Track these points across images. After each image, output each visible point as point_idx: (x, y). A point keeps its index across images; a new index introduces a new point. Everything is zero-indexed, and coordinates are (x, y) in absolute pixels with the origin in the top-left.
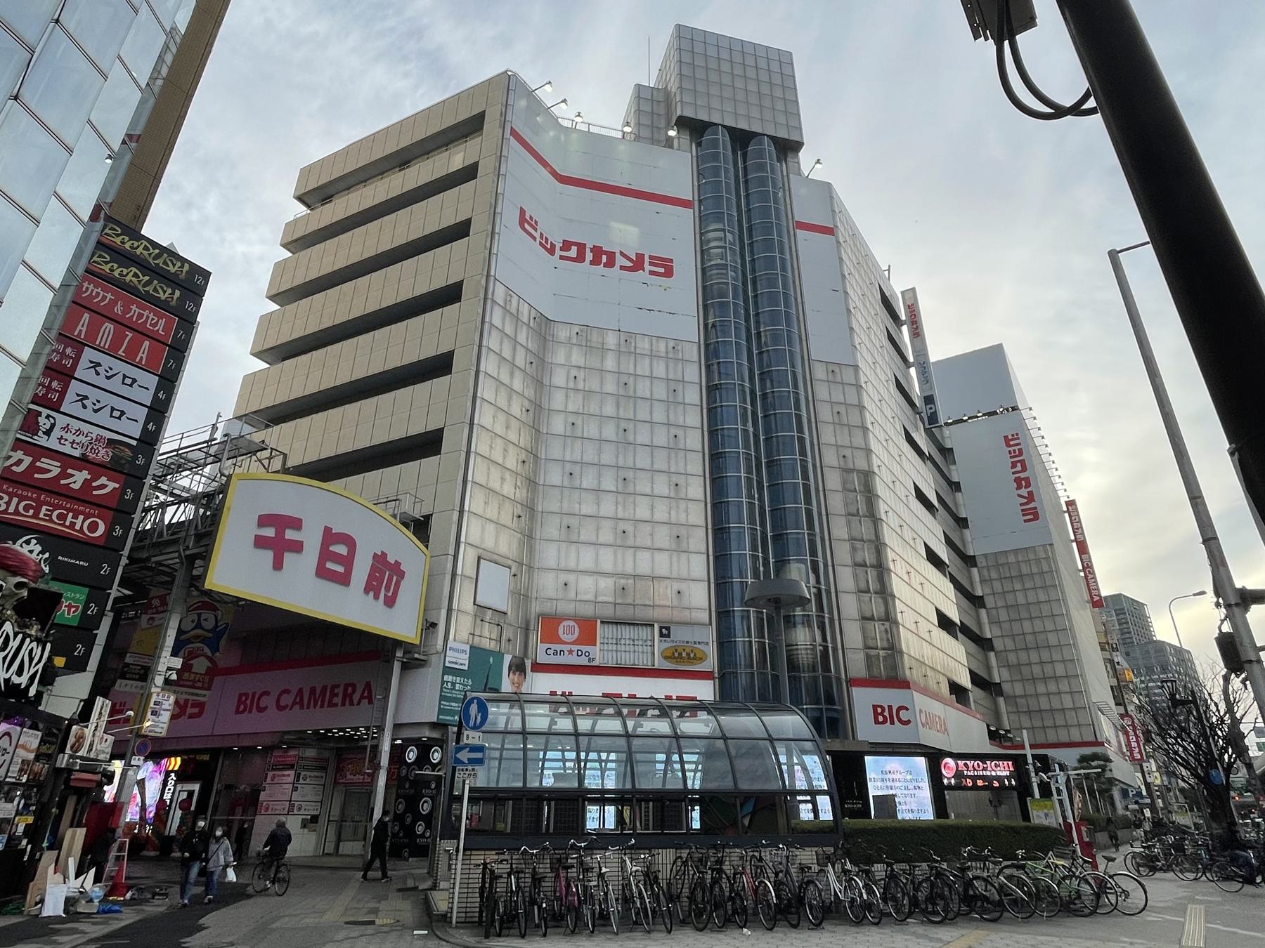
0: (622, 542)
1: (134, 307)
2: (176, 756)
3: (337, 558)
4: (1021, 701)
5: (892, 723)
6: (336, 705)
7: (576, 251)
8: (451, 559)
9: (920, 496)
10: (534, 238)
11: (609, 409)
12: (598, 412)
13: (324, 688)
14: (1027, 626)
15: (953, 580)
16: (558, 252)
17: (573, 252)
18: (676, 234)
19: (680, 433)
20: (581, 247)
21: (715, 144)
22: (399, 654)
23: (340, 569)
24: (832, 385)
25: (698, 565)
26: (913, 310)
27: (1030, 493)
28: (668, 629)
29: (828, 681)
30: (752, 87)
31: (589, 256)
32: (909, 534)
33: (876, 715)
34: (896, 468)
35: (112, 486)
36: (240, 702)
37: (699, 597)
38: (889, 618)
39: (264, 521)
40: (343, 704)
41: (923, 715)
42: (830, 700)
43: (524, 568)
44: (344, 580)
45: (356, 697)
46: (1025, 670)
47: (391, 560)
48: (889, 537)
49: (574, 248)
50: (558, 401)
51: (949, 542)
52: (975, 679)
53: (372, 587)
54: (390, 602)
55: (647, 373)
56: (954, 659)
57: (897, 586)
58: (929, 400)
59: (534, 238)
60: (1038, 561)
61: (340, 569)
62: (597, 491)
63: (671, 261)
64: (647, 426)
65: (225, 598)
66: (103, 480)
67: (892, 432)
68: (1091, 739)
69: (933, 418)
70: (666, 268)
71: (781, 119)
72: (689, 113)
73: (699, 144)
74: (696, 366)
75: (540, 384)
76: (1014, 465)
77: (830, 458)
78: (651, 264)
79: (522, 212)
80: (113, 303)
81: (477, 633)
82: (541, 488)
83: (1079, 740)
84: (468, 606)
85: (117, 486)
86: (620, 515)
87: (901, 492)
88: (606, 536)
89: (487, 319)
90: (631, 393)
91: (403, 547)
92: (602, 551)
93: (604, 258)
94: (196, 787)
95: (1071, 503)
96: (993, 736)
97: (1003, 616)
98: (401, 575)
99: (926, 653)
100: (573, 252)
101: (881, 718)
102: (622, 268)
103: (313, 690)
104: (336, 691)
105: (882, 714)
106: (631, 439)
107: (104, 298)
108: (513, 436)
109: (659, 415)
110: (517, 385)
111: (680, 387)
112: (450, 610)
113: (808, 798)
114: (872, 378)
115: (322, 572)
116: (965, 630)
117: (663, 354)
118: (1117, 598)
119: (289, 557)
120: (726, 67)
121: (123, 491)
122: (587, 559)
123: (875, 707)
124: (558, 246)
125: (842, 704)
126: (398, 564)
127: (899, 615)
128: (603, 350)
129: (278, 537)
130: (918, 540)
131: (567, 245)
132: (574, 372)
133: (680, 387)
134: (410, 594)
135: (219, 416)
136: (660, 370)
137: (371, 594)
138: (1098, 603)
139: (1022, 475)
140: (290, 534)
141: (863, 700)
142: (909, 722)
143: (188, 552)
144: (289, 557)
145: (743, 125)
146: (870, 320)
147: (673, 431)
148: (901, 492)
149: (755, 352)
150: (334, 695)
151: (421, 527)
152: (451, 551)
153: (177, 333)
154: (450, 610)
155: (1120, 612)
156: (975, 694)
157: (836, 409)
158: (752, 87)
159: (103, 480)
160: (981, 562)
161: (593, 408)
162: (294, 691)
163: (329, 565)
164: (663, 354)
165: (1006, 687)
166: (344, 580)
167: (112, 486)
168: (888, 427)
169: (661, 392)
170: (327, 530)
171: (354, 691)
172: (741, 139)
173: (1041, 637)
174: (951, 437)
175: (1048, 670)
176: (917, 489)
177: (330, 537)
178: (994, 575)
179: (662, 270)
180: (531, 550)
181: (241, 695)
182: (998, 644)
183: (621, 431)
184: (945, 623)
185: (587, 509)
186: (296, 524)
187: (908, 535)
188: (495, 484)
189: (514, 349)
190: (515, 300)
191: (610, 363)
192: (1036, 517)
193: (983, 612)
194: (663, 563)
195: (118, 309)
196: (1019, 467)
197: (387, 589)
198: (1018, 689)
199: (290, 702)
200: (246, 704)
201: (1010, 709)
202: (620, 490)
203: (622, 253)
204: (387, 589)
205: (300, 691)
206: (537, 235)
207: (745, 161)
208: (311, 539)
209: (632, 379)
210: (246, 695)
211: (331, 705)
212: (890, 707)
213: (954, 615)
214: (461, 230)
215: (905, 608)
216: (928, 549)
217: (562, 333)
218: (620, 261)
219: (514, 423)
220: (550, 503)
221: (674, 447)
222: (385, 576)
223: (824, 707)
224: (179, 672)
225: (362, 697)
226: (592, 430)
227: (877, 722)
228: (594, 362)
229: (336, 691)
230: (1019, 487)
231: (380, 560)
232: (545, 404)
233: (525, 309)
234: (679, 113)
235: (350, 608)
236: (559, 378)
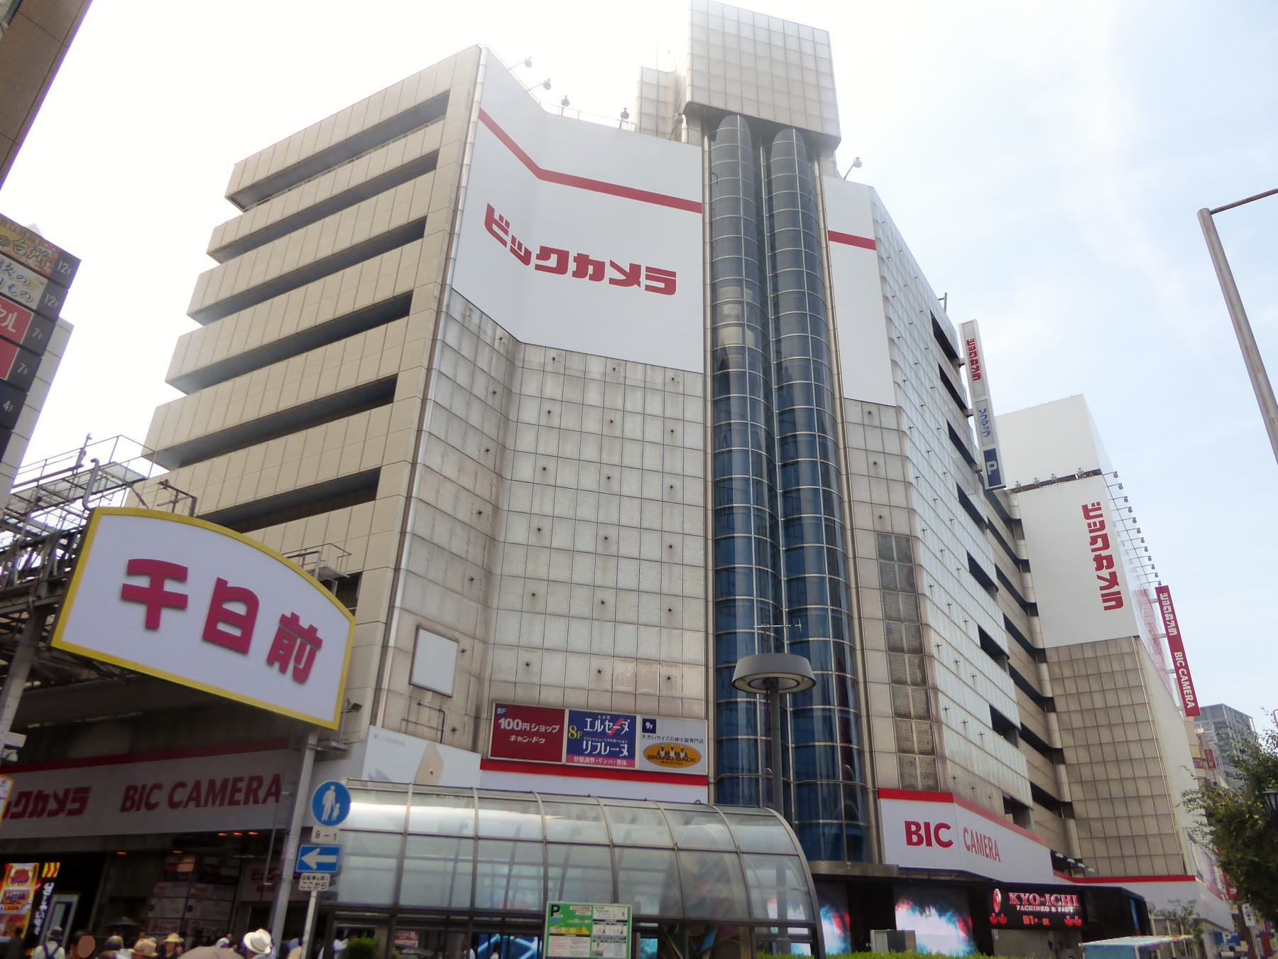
2: (55, 861)
3: (232, 619)
4: (1096, 826)
5: (929, 844)
6: (237, 803)
7: (557, 261)
8: (382, 627)
9: (975, 570)
10: (504, 243)
11: (590, 452)
12: (575, 456)
13: (225, 781)
14: (1105, 735)
15: (1014, 674)
16: (534, 261)
17: (553, 261)
18: (681, 244)
19: (677, 483)
20: (563, 256)
22: (312, 740)
23: (236, 632)
25: (693, 647)
26: (972, 346)
27: (1113, 575)
28: (653, 722)
29: (851, 793)
31: (572, 266)
32: (958, 615)
33: (909, 834)
34: (947, 538)
36: (127, 797)
37: (694, 684)
38: (928, 715)
39: (136, 567)
40: (246, 802)
41: (968, 836)
42: (851, 814)
43: (476, 641)
44: (241, 646)
45: (261, 795)
46: (1102, 788)
47: (304, 624)
48: (931, 616)
49: (554, 258)
50: (526, 440)
51: (1010, 627)
52: (1038, 794)
53: (278, 656)
54: (301, 676)
55: (640, 409)
56: (1014, 769)
57: (940, 676)
58: (991, 455)
59: (504, 243)
60: (1121, 656)
61: (236, 632)
62: (572, 552)
63: (673, 274)
64: (636, 474)
65: (114, 670)
67: (942, 491)
69: (995, 478)
70: (666, 282)
73: (712, 138)
74: (700, 403)
75: (505, 420)
76: (1094, 541)
77: (863, 518)
78: (648, 277)
79: (490, 210)
81: (412, 718)
82: (501, 546)
84: (402, 685)
87: (952, 564)
88: (581, 604)
89: (440, 337)
90: (618, 433)
91: (319, 610)
92: (575, 625)
93: (591, 269)
94: (74, 899)
95: (1162, 590)
96: (1060, 864)
97: (1077, 721)
98: (317, 643)
99: (981, 765)
100: (553, 261)
101: (915, 838)
102: (613, 281)
103: (212, 783)
104: (240, 785)
105: (916, 833)
106: (615, 488)
108: (467, 481)
109: (652, 461)
110: (475, 419)
111: (678, 427)
112: (378, 690)
114: (919, 423)
115: (211, 635)
116: (1028, 736)
117: (659, 387)
118: (1217, 709)
119: (167, 615)
122: (555, 634)
123: (908, 825)
124: (535, 251)
125: (867, 819)
126: (313, 630)
127: (942, 713)
128: (584, 379)
129: (154, 588)
130: (971, 623)
131: (545, 253)
132: (547, 406)
133: (678, 427)
134: (328, 666)
135: (88, 438)
136: (654, 406)
137: (277, 665)
138: (1193, 711)
139: (1104, 553)
140: (171, 586)
141: (893, 817)
142: (949, 844)
143: (37, 603)
144: (167, 615)
146: (918, 354)
147: (669, 480)
148: (952, 564)
149: (774, 387)
150: (236, 790)
151: (345, 588)
152: (383, 618)
154: (378, 690)
155: (1220, 726)
156: (1038, 814)
157: (872, 458)
160: (1051, 656)
161: (569, 449)
162: (190, 785)
163: (222, 627)
164: (659, 387)
165: (1078, 808)
166: (241, 646)
168: (938, 485)
169: (654, 432)
170: (221, 584)
171: (259, 787)
173: (1122, 750)
175: (1130, 789)
176: (972, 561)
177: (223, 592)
178: (1067, 672)
179: (662, 285)
180: (487, 624)
181: (129, 788)
182: (1070, 756)
183: (604, 478)
184: (1001, 725)
185: (559, 573)
186: (179, 573)
187: (957, 615)
188: (441, 539)
189: (473, 373)
190: (476, 317)
191: (593, 396)
192: (1119, 604)
193: (1053, 716)
196: (1100, 543)
197: (298, 660)
198: (1093, 810)
199: (185, 798)
200: (135, 799)
201: (1083, 835)
202: (600, 550)
203: (613, 265)
204: (298, 660)
205: (197, 785)
206: (508, 239)
208: (199, 593)
209: (619, 415)
210: (135, 788)
211: (233, 802)
212: (927, 825)
214: (414, 231)
216: (982, 633)
217: (535, 358)
218: (610, 273)
219: (470, 466)
220: (512, 564)
221: (668, 501)
222: (295, 647)
223: (844, 822)
224: (20, 751)
225: (268, 794)
226: (566, 476)
227: (910, 842)
228: (573, 394)
229: (240, 785)
230: (1099, 568)
231: (289, 625)
232: (510, 443)
233: (489, 328)
234: (688, 98)
235: (246, 679)
236: (529, 412)
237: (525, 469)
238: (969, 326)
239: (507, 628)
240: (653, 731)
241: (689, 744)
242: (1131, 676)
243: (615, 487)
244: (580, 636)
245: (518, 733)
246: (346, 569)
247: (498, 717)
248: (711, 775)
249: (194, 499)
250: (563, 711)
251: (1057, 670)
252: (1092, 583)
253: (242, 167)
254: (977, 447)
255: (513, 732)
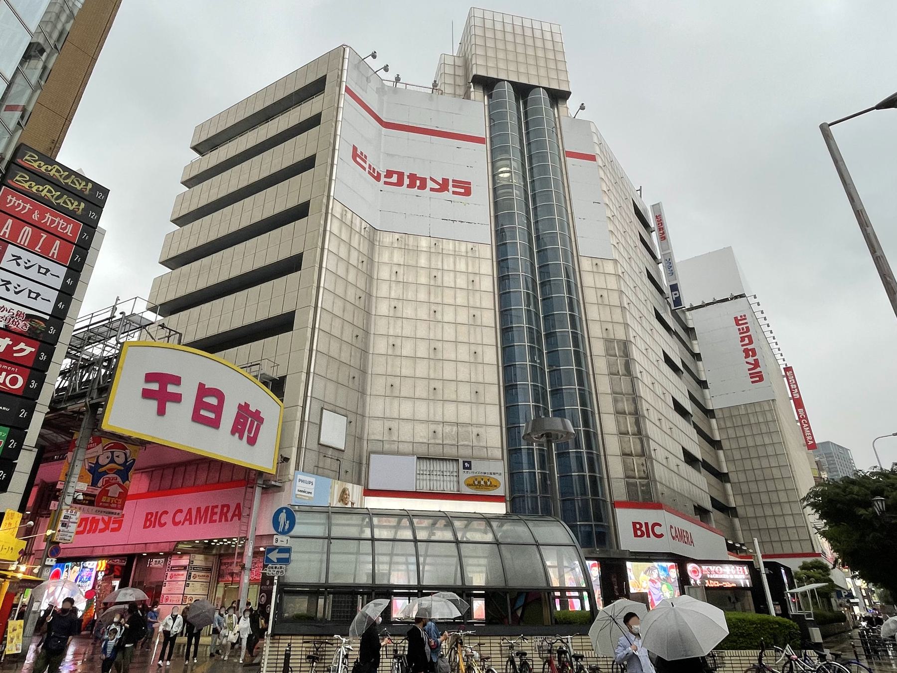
0: (434, 396)
1: (48, 215)
3: (209, 407)
5: (648, 536)
6: (215, 521)
9: (668, 360)
10: (364, 169)
11: (422, 296)
13: (207, 508)
15: (696, 426)
16: (383, 179)
17: (394, 179)
18: (473, 163)
20: (401, 175)
21: (502, 95)
24: (596, 276)
26: (659, 219)
27: (756, 361)
28: (470, 463)
29: (597, 503)
30: (530, 52)
31: (407, 181)
35: (29, 350)
37: (494, 438)
39: (150, 377)
40: (220, 521)
41: (673, 530)
42: (598, 518)
44: (215, 424)
45: (230, 515)
47: (253, 409)
49: (395, 176)
50: (383, 290)
51: (692, 398)
53: (238, 429)
54: (252, 441)
56: (698, 486)
57: (651, 429)
58: (674, 288)
59: (364, 169)
60: (764, 412)
63: (469, 183)
66: (22, 345)
68: (810, 551)
69: (678, 302)
70: (465, 189)
71: (553, 75)
72: (482, 72)
73: (490, 97)
76: (743, 339)
77: (595, 330)
78: (454, 186)
79: (355, 149)
80: (31, 212)
81: (321, 465)
83: (800, 552)
84: (314, 445)
85: (33, 350)
86: (432, 376)
88: (421, 392)
91: (263, 401)
95: (788, 369)
96: (731, 548)
97: (737, 455)
98: (261, 420)
99: (677, 484)
100: (394, 179)
101: (639, 533)
102: (432, 190)
103: (199, 510)
107: (24, 208)
108: (348, 317)
110: (351, 278)
111: (477, 279)
113: (577, 594)
115: (197, 418)
116: (706, 466)
117: (464, 254)
118: (826, 444)
120: (509, 38)
121: (38, 354)
122: (406, 410)
123: (634, 524)
124: (383, 174)
126: (258, 412)
127: (652, 452)
128: (417, 251)
129: (161, 390)
131: (389, 174)
132: (395, 269)
134: (268, 434)
135: (118, 299)
137: (237, 435)
138: (812, 446)
139: (749, 347)
140: (171, 388)
142: (661, 536)
143: (92, 402)
145: (523, 80)
150: (213, 514)
151: (277, 386)
152: (301, 403)
153: (82, 234)
154: (299, 448)
156: (715, 515)
158: (530, 52)
159: (22, 345)
163: (203, 412)
165: (740, 511)
166: (215, 424)
167: (29, 350)
168: (641, 307)
169: (462, 282)
170: (201, 386)
171: (228, 511)
172: (523, 91)
174: (692, 319)
177: (203, 391)
178: (729, 424)
179: (462, 191)
181: (147, 514)
182: (732, 476)
183: (432, 312)
184: (690, 459)
186: (176, 381)
187: (659, 390)
190: (349, 214)
192: (761, 379)
194: (465, 414)
195: (36, 216)
196: (747, 341)
198: (750, 512)
200: (152, 520)
203: (432, 179)
205: (190, 510)
206: (367, 166)
207: (525, 108)
208: (188, 391)
210: (152, 514)
211: (212, 521)
212: (646, 524)
213: (697, 453)
215: (657, 447)
217: (387, 239)
219: (349, 307)
220: (377, 366)
222: (247, 423)
223: (593, 523)
226: (409, 312)
227: (636, 535)
229: (216, 510)
230: (747, 356)
231: (244, 409)
233: (357, 221)
234: (474, 73)
235: (220, 444)
237: (383, 308)
238: (657, 207)
239: (375, 407)
240: (470, 468)
241: (493, 476)
242: (771, 425)
243: (439, 317)
244: (422, 410)
246: (276, 374)
248: (508, 495)
249: (181, 335)
251: (722, 423)
252: (743, 367)
253: (200, 128)
254: (665, 284)
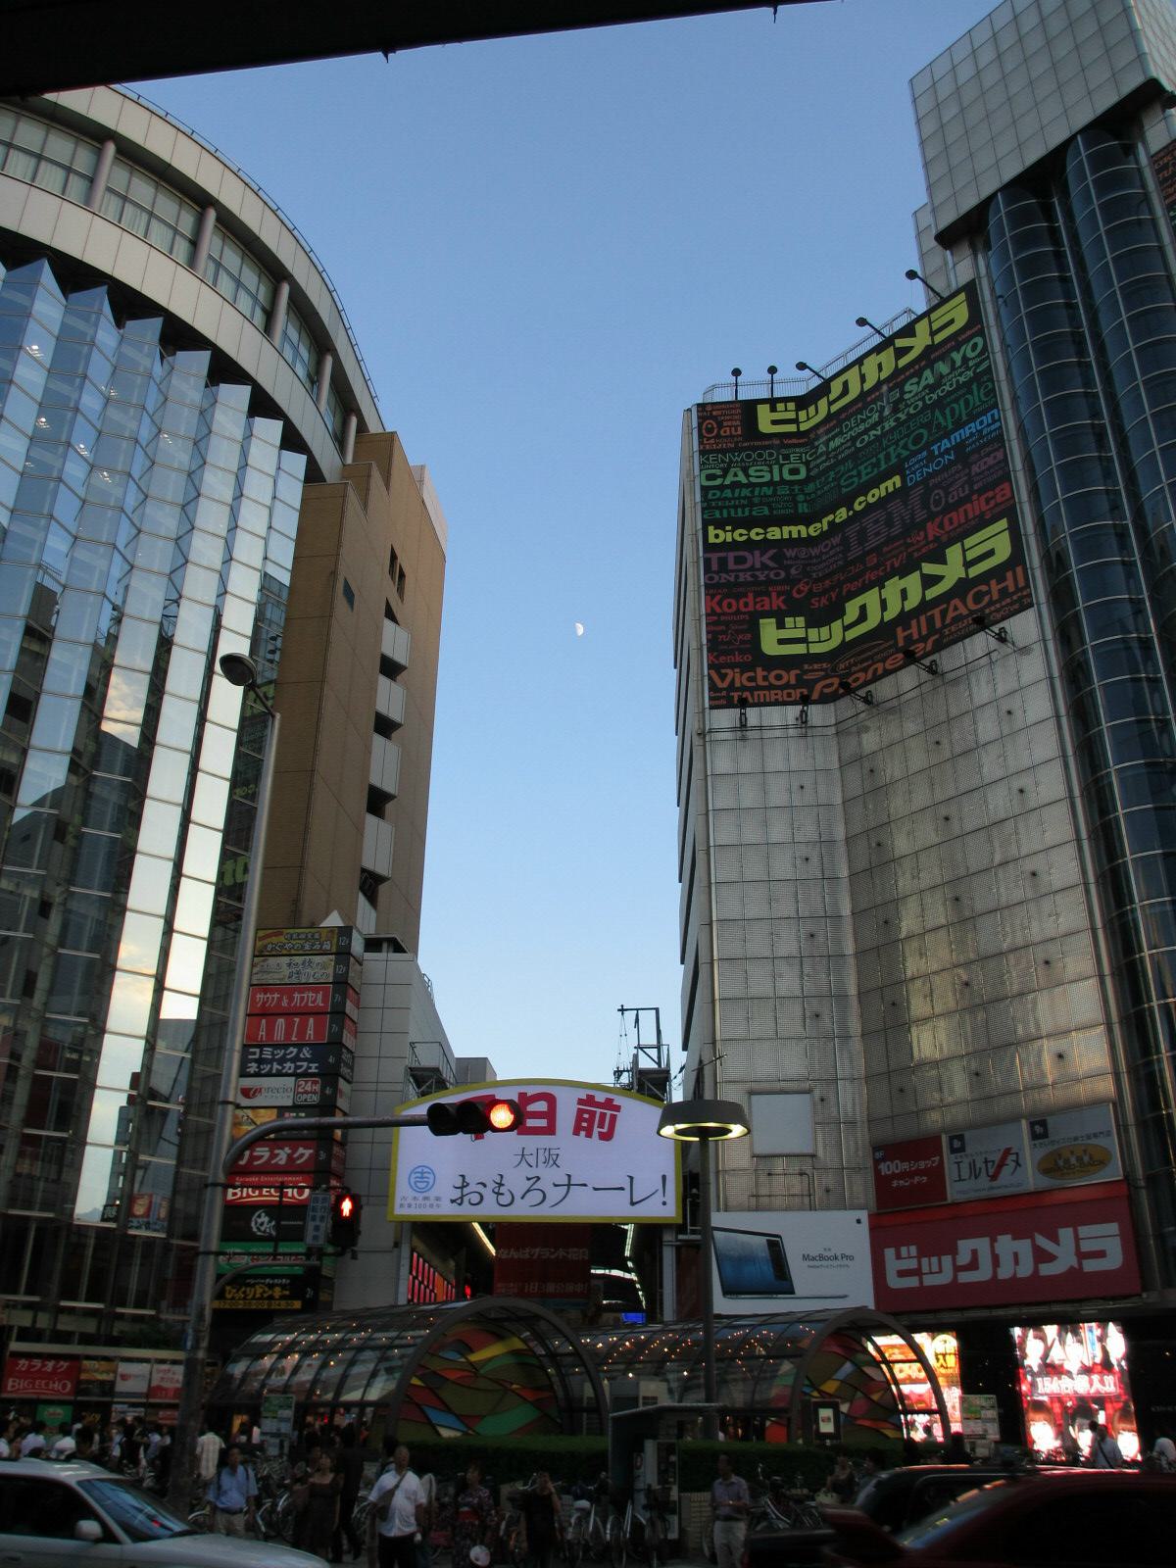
35: (308, 1152)
85: (311, 1151)
167: (308, 1152)
240: (1045, 1135)
241: (1094, 1141)
245: (902, 1176)
247: (877, 1162)
250: (938, 1139)
255: (894, 1176)
